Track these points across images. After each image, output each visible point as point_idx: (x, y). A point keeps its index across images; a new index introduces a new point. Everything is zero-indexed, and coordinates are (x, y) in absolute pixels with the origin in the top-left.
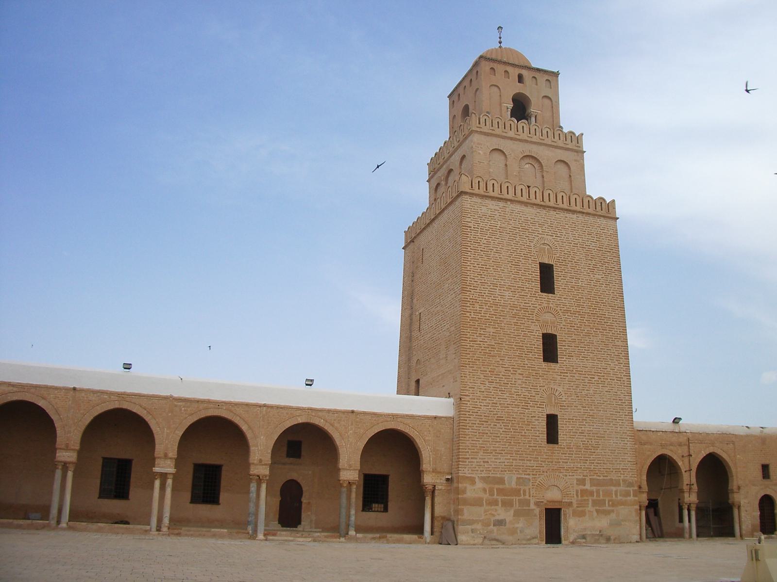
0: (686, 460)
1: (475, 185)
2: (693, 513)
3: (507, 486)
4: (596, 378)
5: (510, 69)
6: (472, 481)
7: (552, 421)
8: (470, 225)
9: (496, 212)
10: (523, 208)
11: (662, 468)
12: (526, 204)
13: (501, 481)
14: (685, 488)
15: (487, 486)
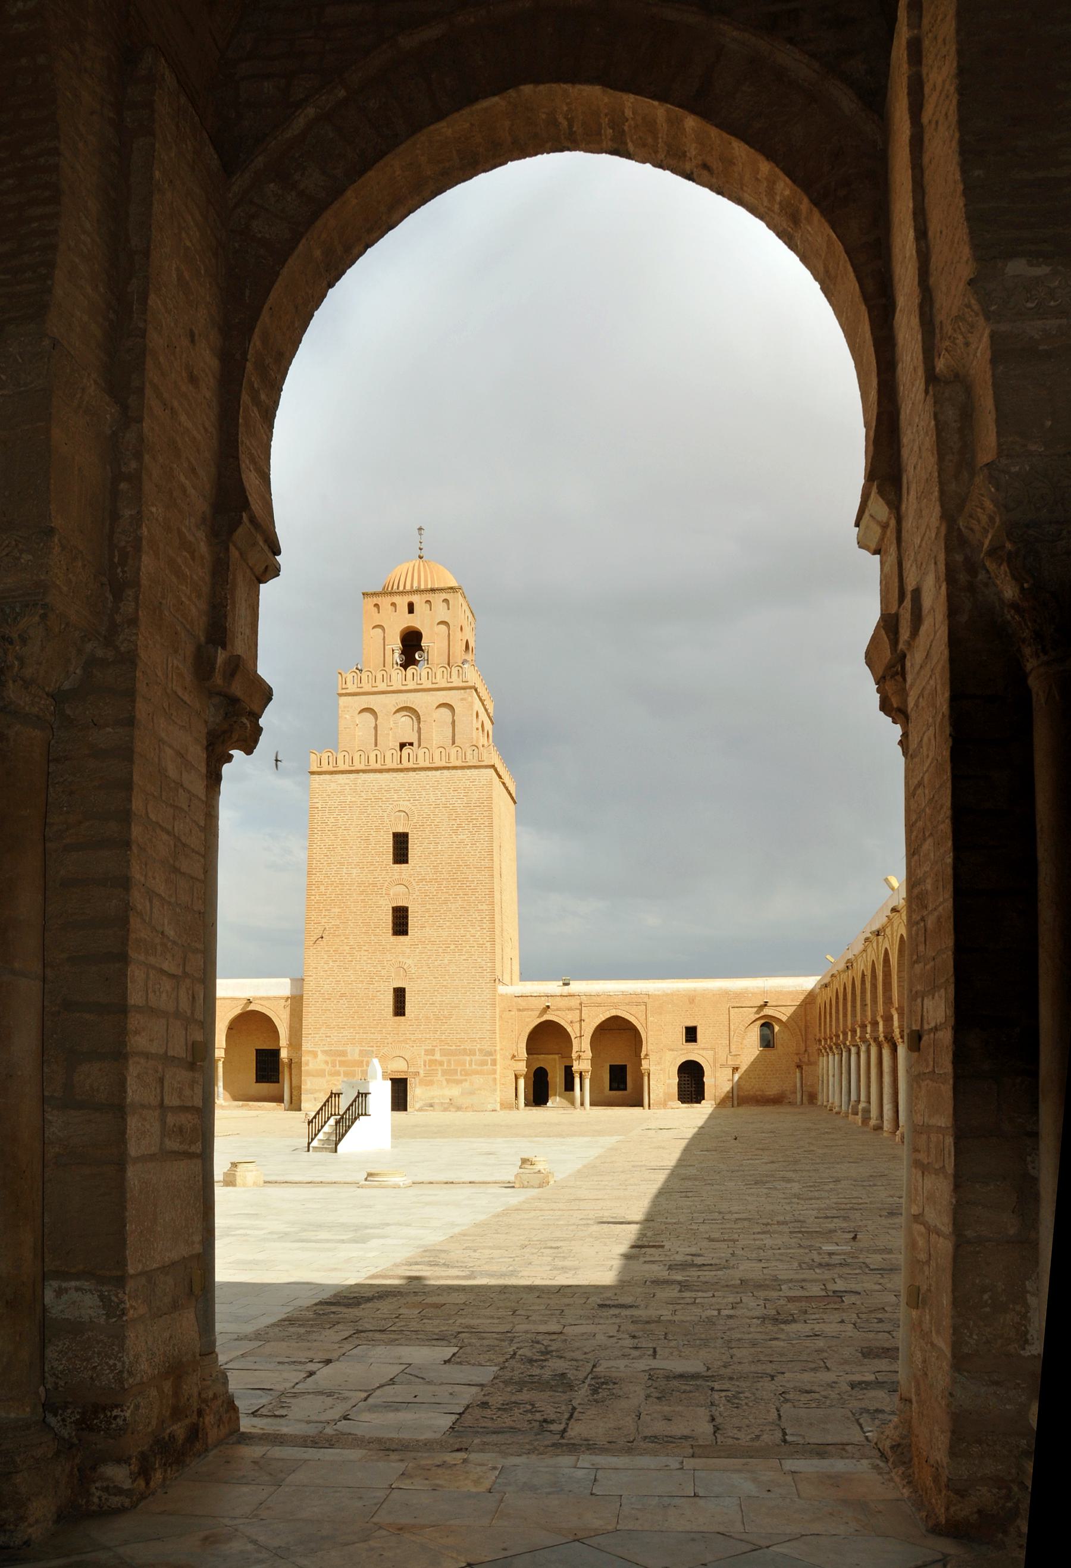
0: (578, 1025)
1: (325, 762)
2: (587, 1083)
3: (349, 1057)
4: (452, 947)
5: (397, 599)
6: (315, 1054)
7: (400, 995)
8: (317, 805)
9: (347, 787)
10: (378, 775)
11: (547, 1037)
12: (380, 771)
13: (343, 1053)
14: (574, 1055)
15: (329, 1059)
